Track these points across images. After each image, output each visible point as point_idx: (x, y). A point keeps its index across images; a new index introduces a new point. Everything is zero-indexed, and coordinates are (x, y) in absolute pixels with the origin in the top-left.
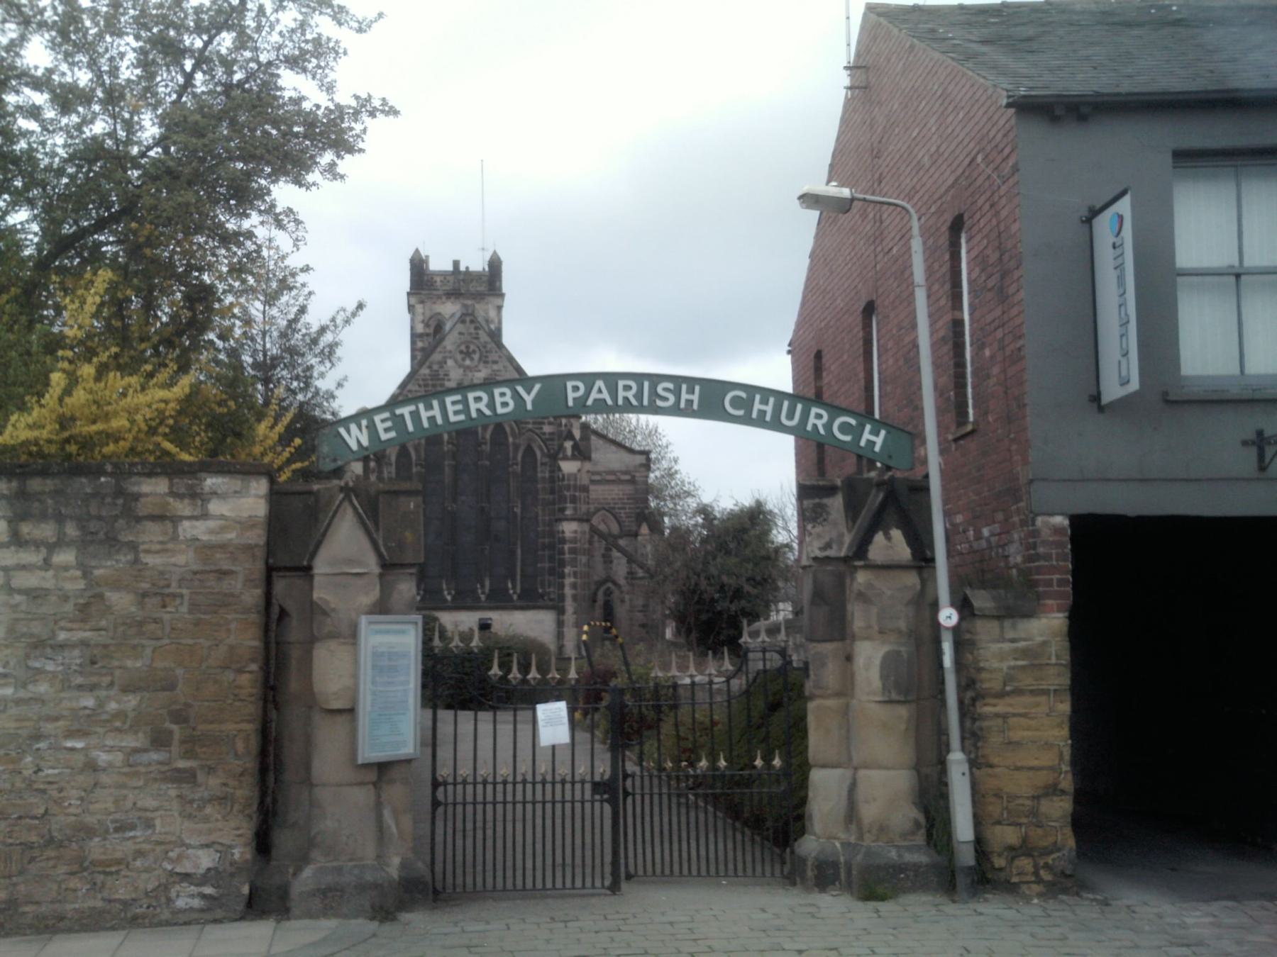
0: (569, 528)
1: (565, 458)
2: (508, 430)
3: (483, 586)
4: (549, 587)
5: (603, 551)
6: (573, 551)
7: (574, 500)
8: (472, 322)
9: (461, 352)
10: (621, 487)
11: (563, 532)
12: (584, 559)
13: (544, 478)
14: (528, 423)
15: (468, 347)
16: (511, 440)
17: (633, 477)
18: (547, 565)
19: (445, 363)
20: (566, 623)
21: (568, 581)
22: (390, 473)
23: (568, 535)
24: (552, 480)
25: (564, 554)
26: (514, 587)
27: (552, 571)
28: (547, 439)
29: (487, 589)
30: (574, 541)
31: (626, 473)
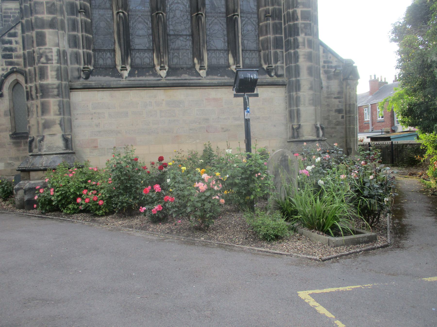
3: (201, 60)
4: (276, 61)
18: (271, 36)
20: (302, 99)
26: (236, 61)
27: (278, 44)
29: (206, 64)
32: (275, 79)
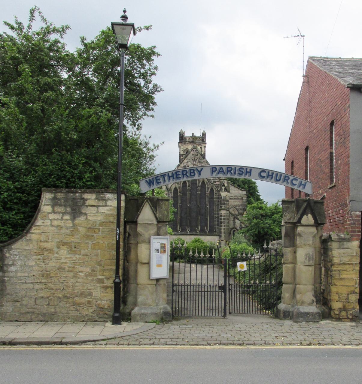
0: (223, 212)
1: (222, 192)
2: (206, 183)
3: (198, 229)
4: (217, 229)
5: (233, 219)
6: (224, 219)
7: (225, 204)
8: (196, 151)
9: (193, 160)
10: (239, 201)
11: (221, 213)
12: (227, 221)
13: (216, 197)
14: (212, 181)
15: (195, 158)
16: (207, 186)
17: (242, 198)
19: (188, 163)
21: (223, 228)
22: (171, 195)
23: (223, 214)
24: (218, 198)
25: (221, 220)
26: (207, 229)
27: (218, 225)
28: (217, 186)
29: (199, 230)
30: (225, 216)
31: (240, 196)
32: (217, 234)
